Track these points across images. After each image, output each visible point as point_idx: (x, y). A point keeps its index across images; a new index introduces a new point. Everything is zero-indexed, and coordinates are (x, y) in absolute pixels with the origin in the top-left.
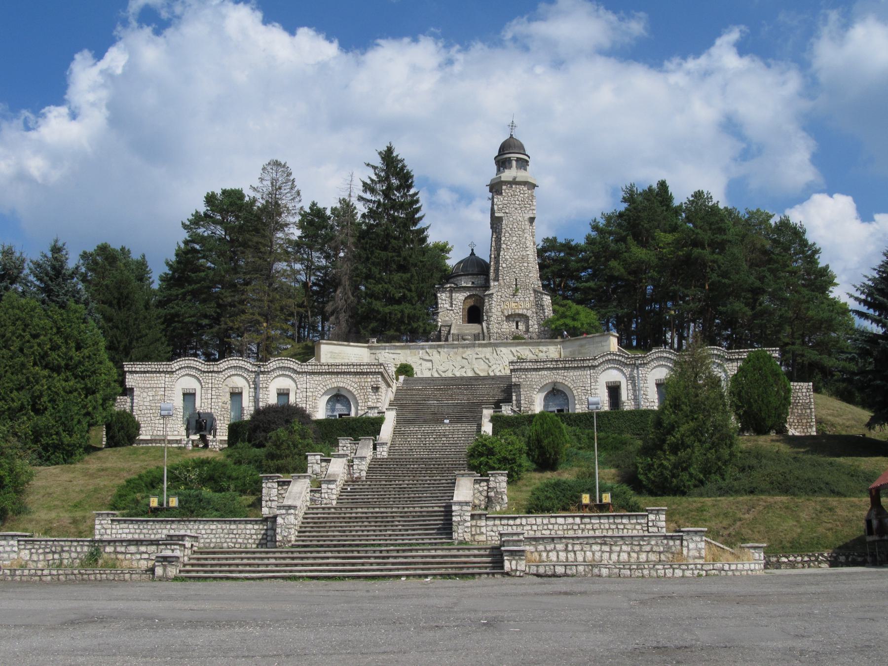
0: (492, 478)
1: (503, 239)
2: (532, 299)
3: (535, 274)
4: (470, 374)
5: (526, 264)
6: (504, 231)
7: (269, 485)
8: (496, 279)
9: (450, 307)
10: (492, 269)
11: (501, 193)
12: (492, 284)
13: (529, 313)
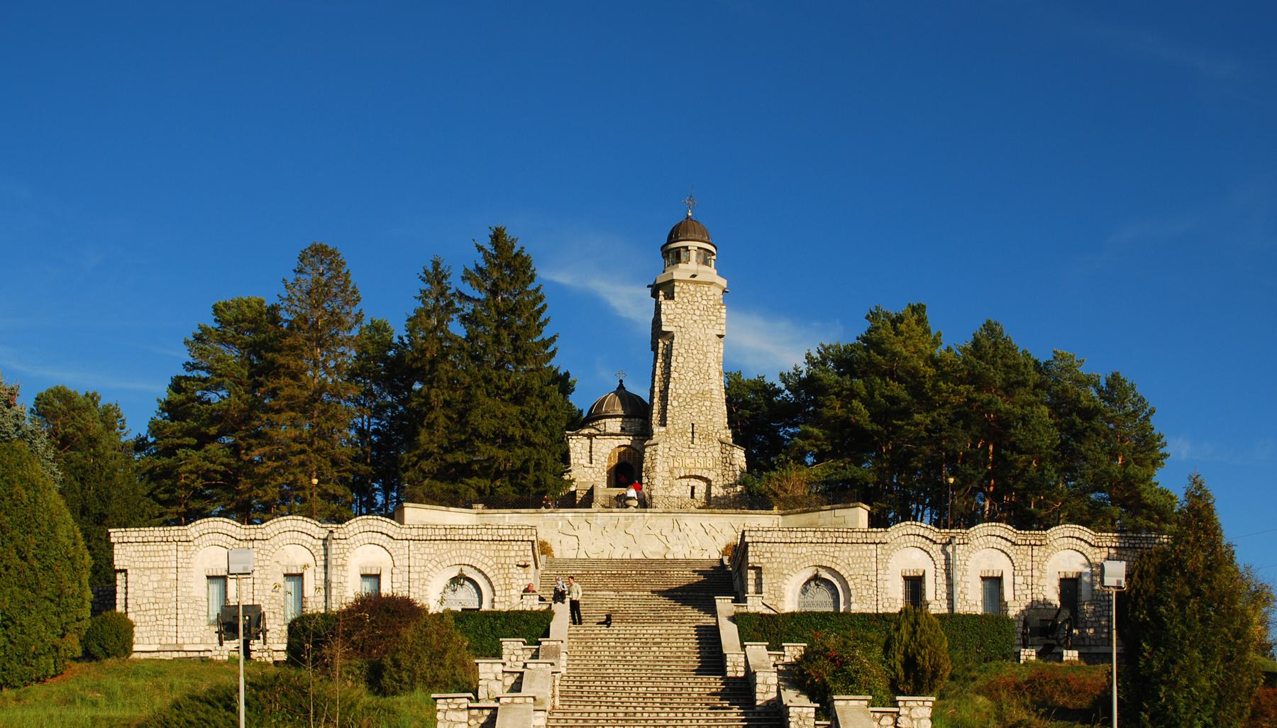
0: (903, 711)
1: (674, 364)
2: (717, 454)
4: (638, 556)
5: (707, 403)
6: (675, 353)
7: (452, 715)
8: (663, 423)
10: (656, 408)
11: (673, 298)
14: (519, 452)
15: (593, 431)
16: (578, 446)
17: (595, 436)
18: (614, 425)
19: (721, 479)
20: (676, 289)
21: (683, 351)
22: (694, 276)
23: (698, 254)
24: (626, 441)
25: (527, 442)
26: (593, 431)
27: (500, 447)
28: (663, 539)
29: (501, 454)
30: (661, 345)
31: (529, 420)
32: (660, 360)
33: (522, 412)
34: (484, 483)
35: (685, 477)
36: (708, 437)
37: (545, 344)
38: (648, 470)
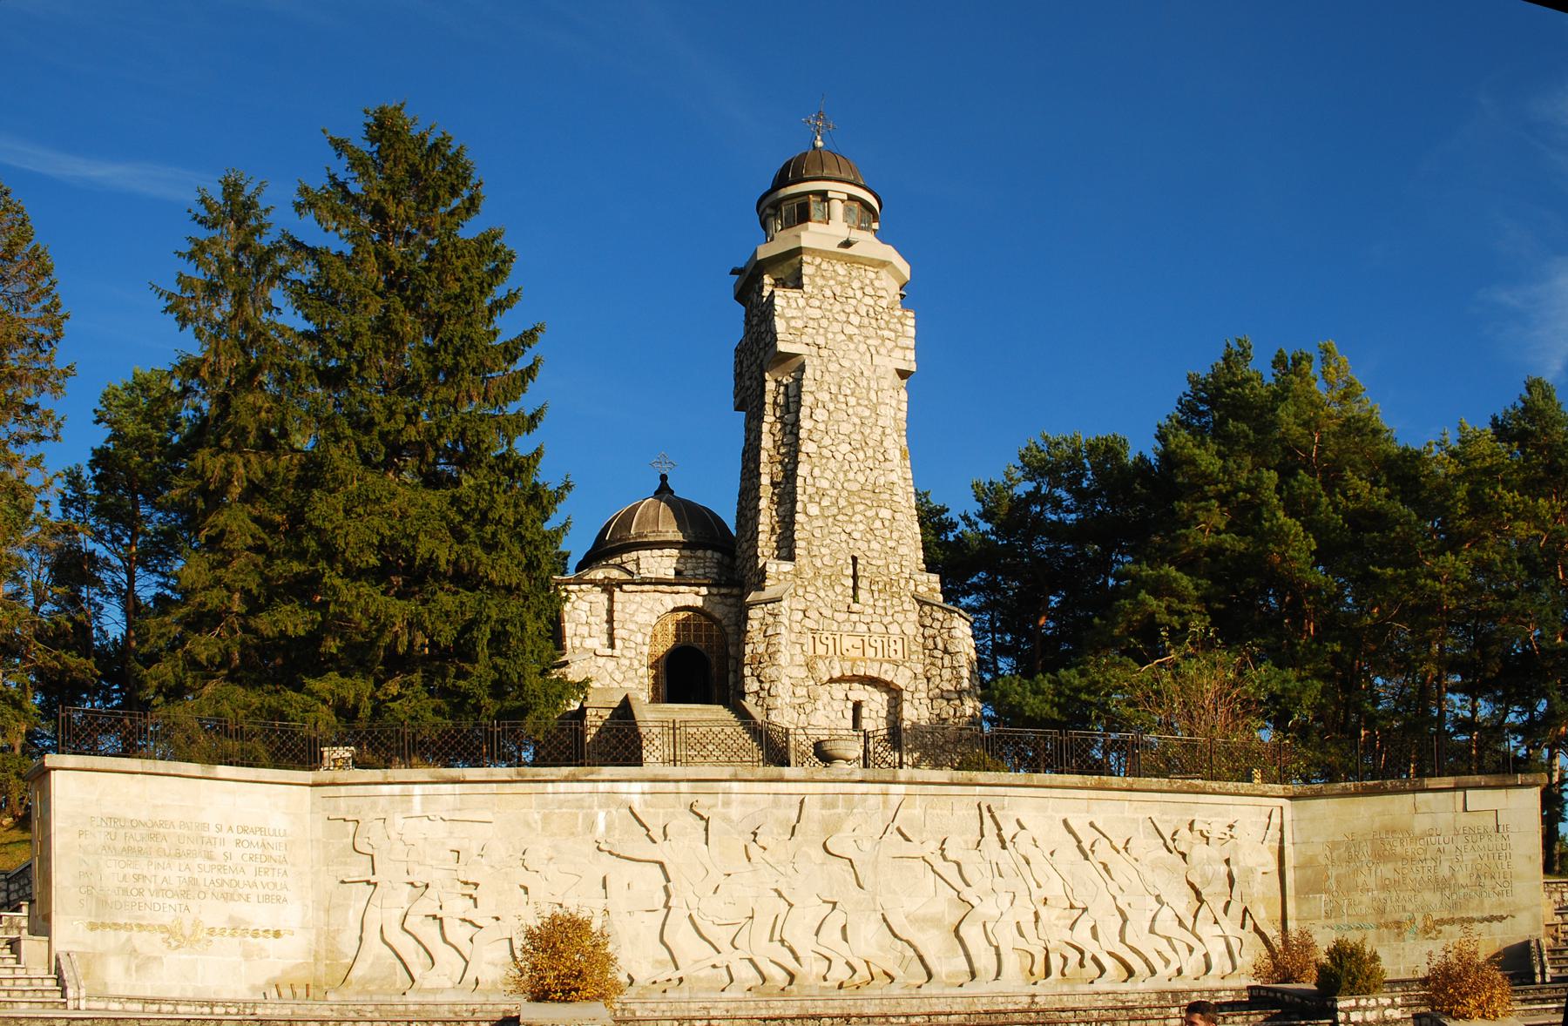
1: (806, 424)
2: (911, 629)
5: (885, 513)
6: (807, 400)
8: (786, 549)
9: (612, 639)
13: (901, 679)
14: (446, 601)
15: (615, 574)
16: (582, 611)
18: (661, 563)
19: (923, 686)
20: (806, 270)
21: (827, 397)
22: (847, 244)
23: (848, 211)
24: (692, 597)
25: (465, 579)
27: (399, 596)
28: (950, 872)
29: (400, 610)
30: (770, 385)
31: (471, 521)
32: (769, 418)
33: (455, 501)
34: (357, 688)
35: (841, 680)
37: (511, 352)
38: (758, 661)
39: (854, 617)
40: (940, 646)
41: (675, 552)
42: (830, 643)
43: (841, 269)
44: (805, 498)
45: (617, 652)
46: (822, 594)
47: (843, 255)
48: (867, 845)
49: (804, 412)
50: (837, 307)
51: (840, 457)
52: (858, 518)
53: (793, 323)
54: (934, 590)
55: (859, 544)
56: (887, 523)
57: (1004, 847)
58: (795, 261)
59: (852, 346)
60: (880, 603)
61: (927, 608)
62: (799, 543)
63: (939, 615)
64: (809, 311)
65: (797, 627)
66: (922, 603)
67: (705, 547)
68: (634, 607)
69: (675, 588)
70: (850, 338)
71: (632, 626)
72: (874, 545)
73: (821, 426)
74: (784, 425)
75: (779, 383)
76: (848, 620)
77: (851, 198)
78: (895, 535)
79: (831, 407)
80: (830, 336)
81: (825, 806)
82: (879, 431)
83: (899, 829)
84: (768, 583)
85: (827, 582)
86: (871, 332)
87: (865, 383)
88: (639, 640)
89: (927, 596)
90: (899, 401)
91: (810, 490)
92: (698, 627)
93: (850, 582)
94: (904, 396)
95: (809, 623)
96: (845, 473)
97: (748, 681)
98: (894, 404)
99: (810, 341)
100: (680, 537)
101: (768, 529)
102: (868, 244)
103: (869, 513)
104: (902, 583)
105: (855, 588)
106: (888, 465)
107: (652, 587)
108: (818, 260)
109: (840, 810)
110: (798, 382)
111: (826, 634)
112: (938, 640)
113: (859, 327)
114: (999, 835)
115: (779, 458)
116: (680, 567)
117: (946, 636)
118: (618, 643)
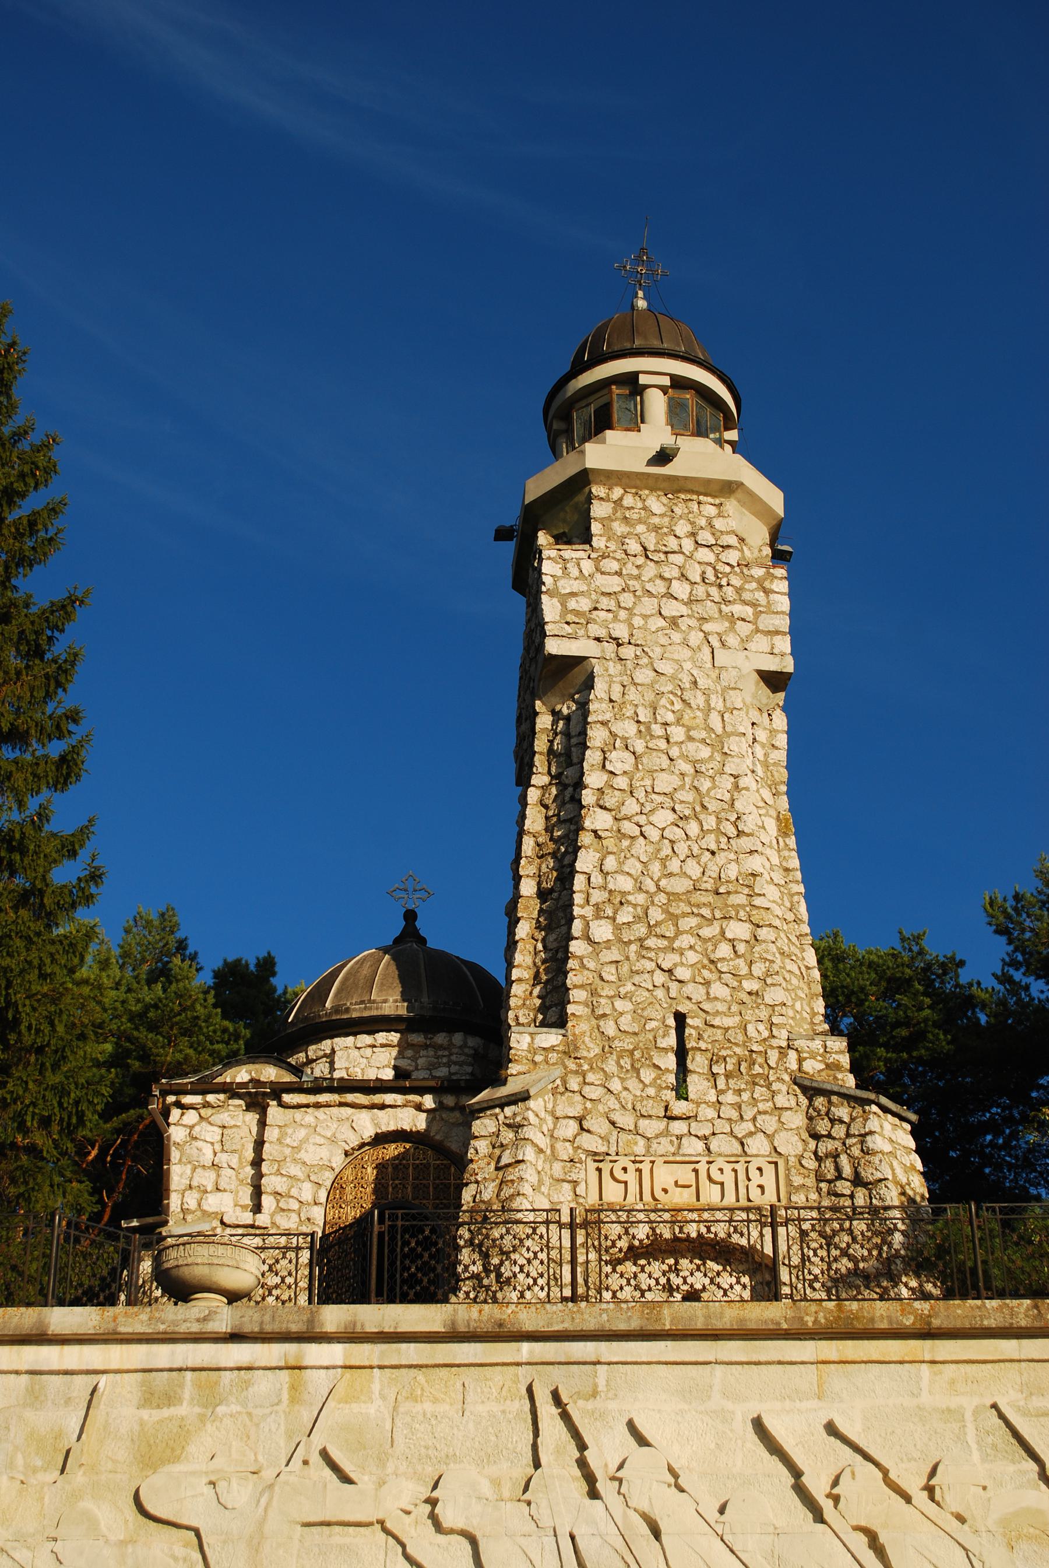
1: (593, 779)
2: (791, 1144)
3: (798, 996)
5: (738, 930)
6: (596, 736)
8: (554, 1010)
11: (586, 538)
12: (520, 1041)
17: (277, 1091)
20: (598, 510)
21: (628, 729)
24: (408, 1115)
26: (270, 1073)
30: (544, 721)
32: (540, 779)
36: (747, 1069)
38: (483, 1216)
39: (679, 1127)
40: (847, 1171)
41: (394, 1037)
42: (631, 1177)
43: (656, 504)
44: (588, 912)
45: (262, 1219)
46: (616, 1085)
47: (657, 477)
48: (240, 1494)
49: (592, 757)
50: (650, 570)
51: (654, 834)
52: (685, 941)
53: (572, 604)
54: (836, 1067)
55: (689, 989)
56: (741, 948)
57: (594, 1494)
58: (581, 498)
59: (677, 637)
60: (730, 1098)
61: (820, 1101)
62: (576, 995)
63: (843, 1112)
64: (600, 580)
65: (565, 1151)
66: (810, 1090)
67: (450, 1028)
68: (302, 1133)
69: (378, 1098)
70: (674, 622)
71: (295, 1170)
72: (718, 990)
73: (622, 782)
74: (562, 786)
75: (556, 714)
76: (666, 1133)
77: (679, 383)
78: (758, 969)
79: (639, 746)
80: (637, 621)
81: (150, 1399)
82: (727, 783)
83: (324, 1454)
84: (513, 1069)
85: (626, 1062)
86: (710, 609)
87: (700, 700)
88: (307, 1195)
89: (824, 1080)
90: (773, 732)
91: (597, 896)
92: (422, 1170)
93: (670, 1062)
94: (780, 721)
95: (589, 1142)
96: (664, 861)
97: (465, 1256)
98: (761, 739)
99: (602, 633)
100: (402, 1010)
101: (527, 975)
102: (705, 457)
103: (707, 932)
104: (773, 1057)
105: (682, 1070)
106: (745, 843)
107: (334, 1098)
108: (617, 492)
109: (184, 1410)
110: (583, 707)
111: (623, 1161)
112: (844, 1160)
113: (690, 602)
114: (582, 1463)
115: (552, 846)
116: (404, 1064)
117: (856, 1151)
118: (267, 1201)
